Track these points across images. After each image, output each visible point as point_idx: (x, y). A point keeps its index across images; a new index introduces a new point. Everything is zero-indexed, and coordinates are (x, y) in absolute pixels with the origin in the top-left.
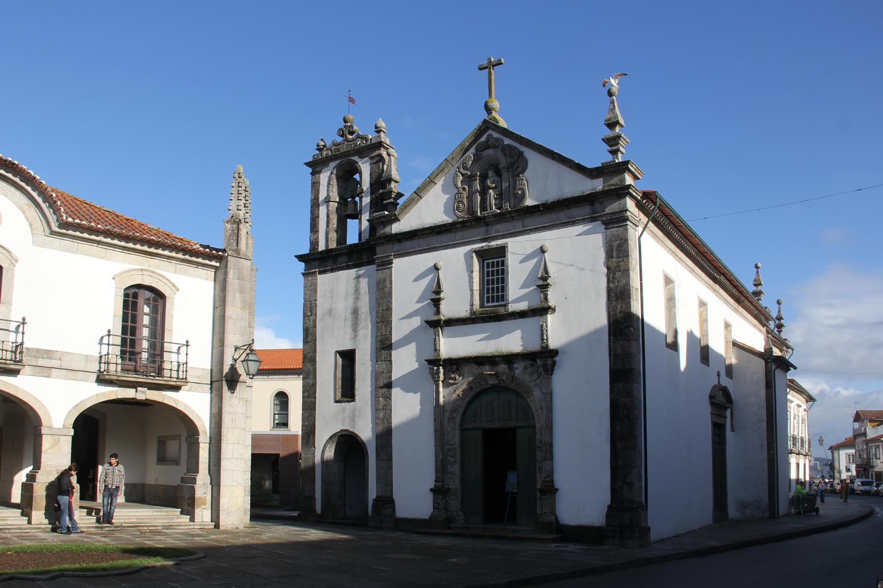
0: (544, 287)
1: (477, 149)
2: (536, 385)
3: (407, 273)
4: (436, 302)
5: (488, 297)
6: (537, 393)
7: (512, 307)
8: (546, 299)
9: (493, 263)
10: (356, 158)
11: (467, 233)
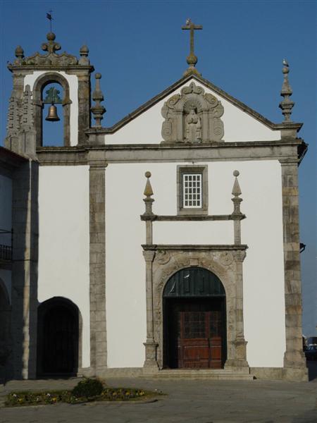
0: (237, 202)
1: (182, 91)
2: (229, 268)
3: (123, 181)
4: (149, 202)
5: (186, 202)
6: (231, 275)
7: (211, 213)
8: (239, 209)
9: (190, 177)
10: (62, 73)
11: (174, 153)
